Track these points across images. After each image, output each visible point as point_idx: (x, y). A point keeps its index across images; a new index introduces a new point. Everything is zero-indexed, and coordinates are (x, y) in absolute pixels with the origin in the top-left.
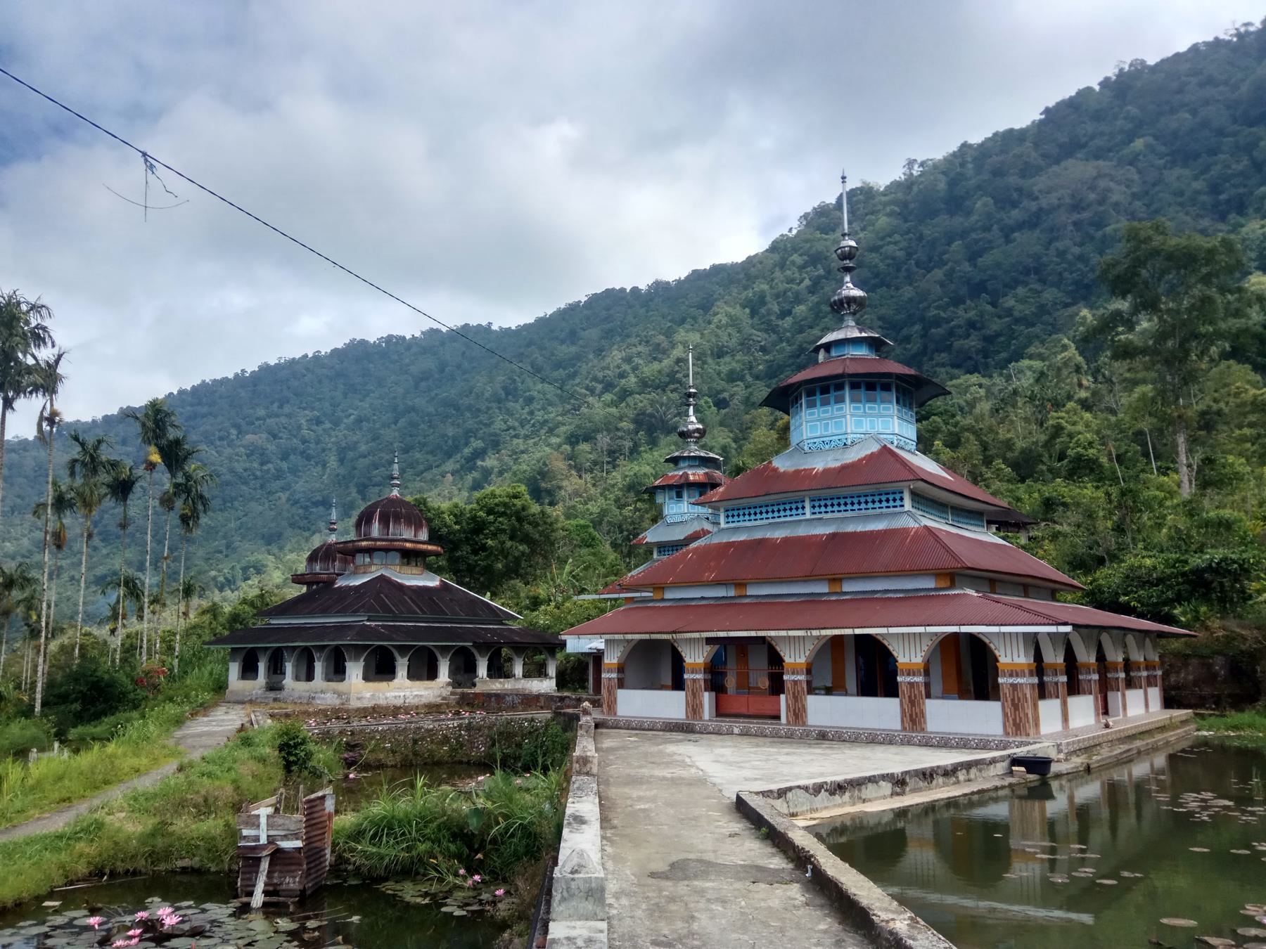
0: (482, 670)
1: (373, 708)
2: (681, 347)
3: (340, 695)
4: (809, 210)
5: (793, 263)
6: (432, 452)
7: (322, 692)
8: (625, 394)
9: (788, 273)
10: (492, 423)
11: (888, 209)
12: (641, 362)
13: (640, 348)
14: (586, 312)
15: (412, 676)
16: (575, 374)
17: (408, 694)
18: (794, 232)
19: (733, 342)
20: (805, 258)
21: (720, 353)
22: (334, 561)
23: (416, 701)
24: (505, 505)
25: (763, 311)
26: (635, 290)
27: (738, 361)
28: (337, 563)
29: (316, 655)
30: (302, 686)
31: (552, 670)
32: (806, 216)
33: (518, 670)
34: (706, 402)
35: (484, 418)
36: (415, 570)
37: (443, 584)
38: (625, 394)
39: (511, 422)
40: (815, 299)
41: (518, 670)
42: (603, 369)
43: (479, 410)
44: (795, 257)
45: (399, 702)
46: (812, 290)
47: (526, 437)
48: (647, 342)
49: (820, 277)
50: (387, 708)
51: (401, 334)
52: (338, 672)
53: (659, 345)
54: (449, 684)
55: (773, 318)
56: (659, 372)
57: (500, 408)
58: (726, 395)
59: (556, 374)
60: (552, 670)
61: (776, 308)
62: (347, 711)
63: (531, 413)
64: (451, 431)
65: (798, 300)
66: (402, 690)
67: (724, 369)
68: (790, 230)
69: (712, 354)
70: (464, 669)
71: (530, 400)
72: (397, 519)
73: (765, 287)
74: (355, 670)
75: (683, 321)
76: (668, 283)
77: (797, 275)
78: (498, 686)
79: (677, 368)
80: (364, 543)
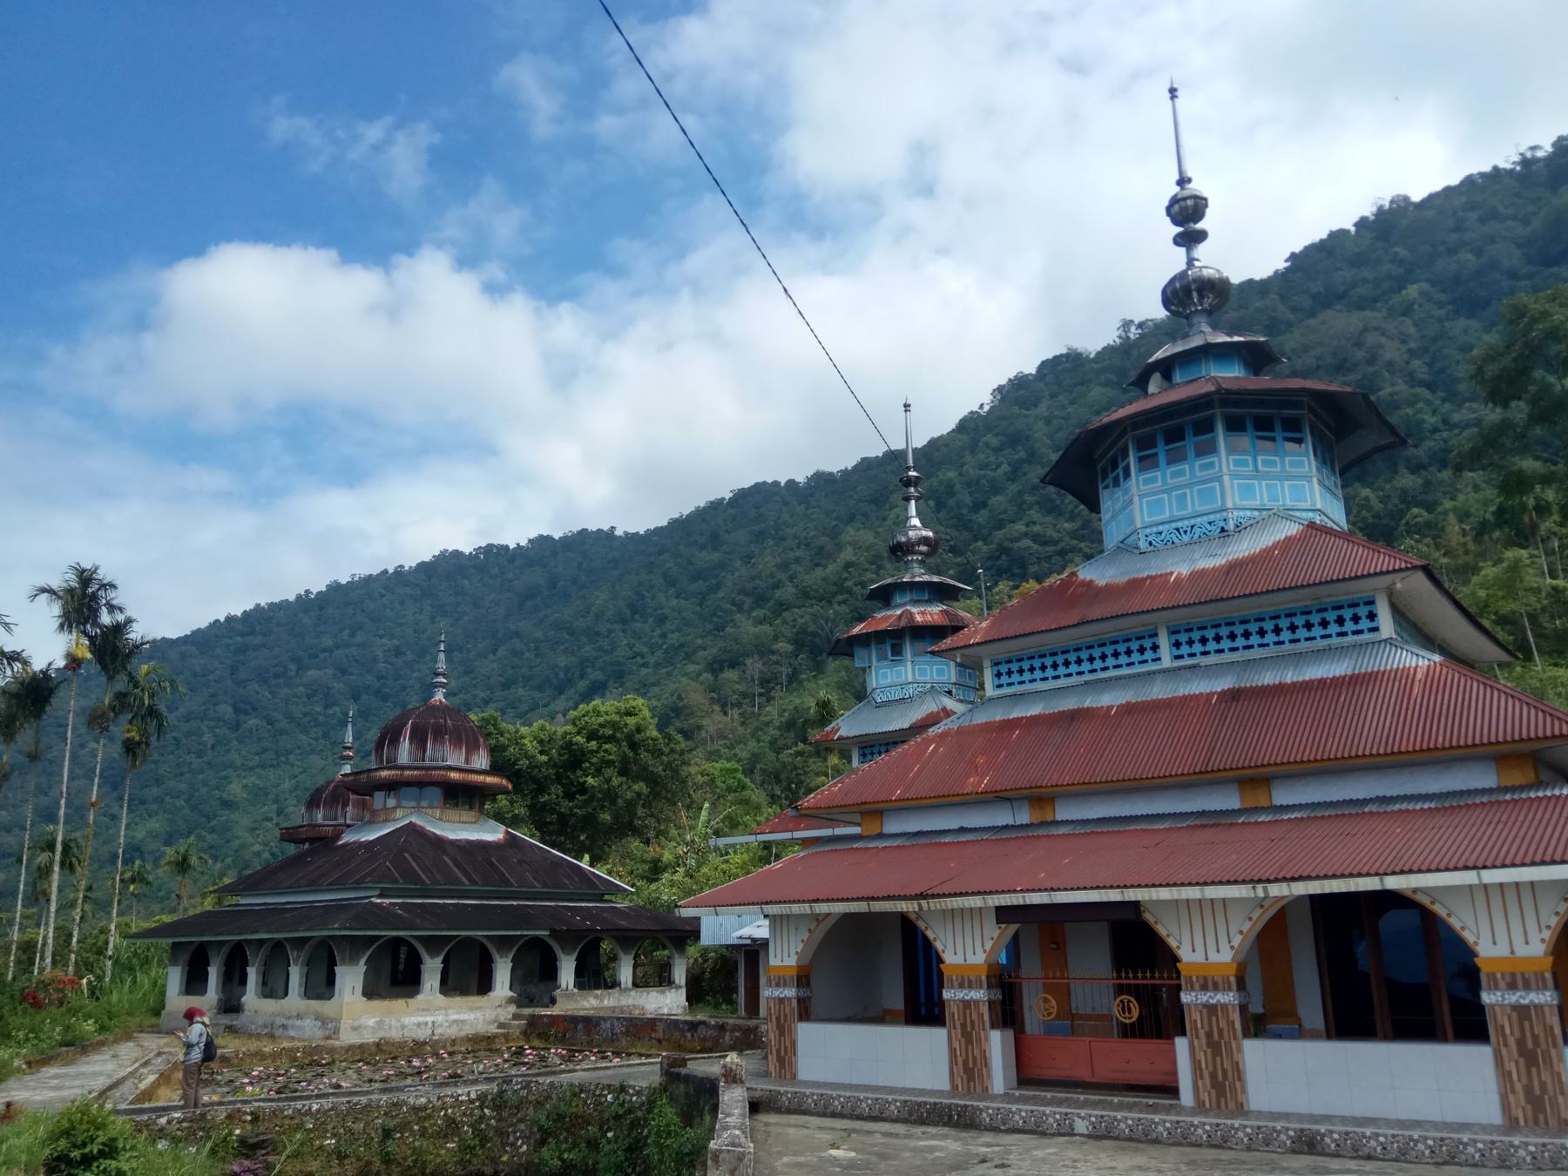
1: (378, 1045)
2: (849, 549)
3: (323, 1020)
4: (1004, 381)
5: (987, 445)
6: (539, 688)
7: (299, 1017)
8: (782, 607)
9: (981, 456)
10: (613, 650)
11: (1102, 378)
13: (799, 553)
14: (732, 511)
15: (450, 986)
16: (718, 586)
17: (440, 1018)
18: (986, 408)
22: (345, 805)
23: (453, 1032)
24: (614, 725)
25: (951, 502)
26: (791, 483)
28: (350, 809)
29: (292, 955)
30: (270, 1005)
31: (680, 974)
32: (1000, 389)
33: (626, 974)
35: (605, 643)
36: (466, 815)
37: (511, 841)
38: (782, 607)
39: (638, 647)
40: (1014, 488)
41: (626, 974)
42: (753, 579)
43: (598, 634)
44: (989, 438)
45: (422, 1035)
46: (1013, 476)
47: (657, 665)
48: (807, 545)
49: (1022, 461)
50: (402, 1045)
52: (322, 985)
53: (822, 548)
54: (510, 1001)
56: (824, 579)
57: (624, 631)
59: (694, 587)
60: (680, 974)
61: (967, 499)
62: (331, 1051)
63: (664, 636)
64: (562, 661)
65: (996, 489)
66: (433, 1014)
68: (981, 406)
71: (662, 620)
72: (439, 734)
73: (952, 474)
74: (350, 978)
75: (851, 519)
76: (831, 474)
77: (992, 459)
78: (592, 1003)
79: (845, 575)
80: (384, 773)
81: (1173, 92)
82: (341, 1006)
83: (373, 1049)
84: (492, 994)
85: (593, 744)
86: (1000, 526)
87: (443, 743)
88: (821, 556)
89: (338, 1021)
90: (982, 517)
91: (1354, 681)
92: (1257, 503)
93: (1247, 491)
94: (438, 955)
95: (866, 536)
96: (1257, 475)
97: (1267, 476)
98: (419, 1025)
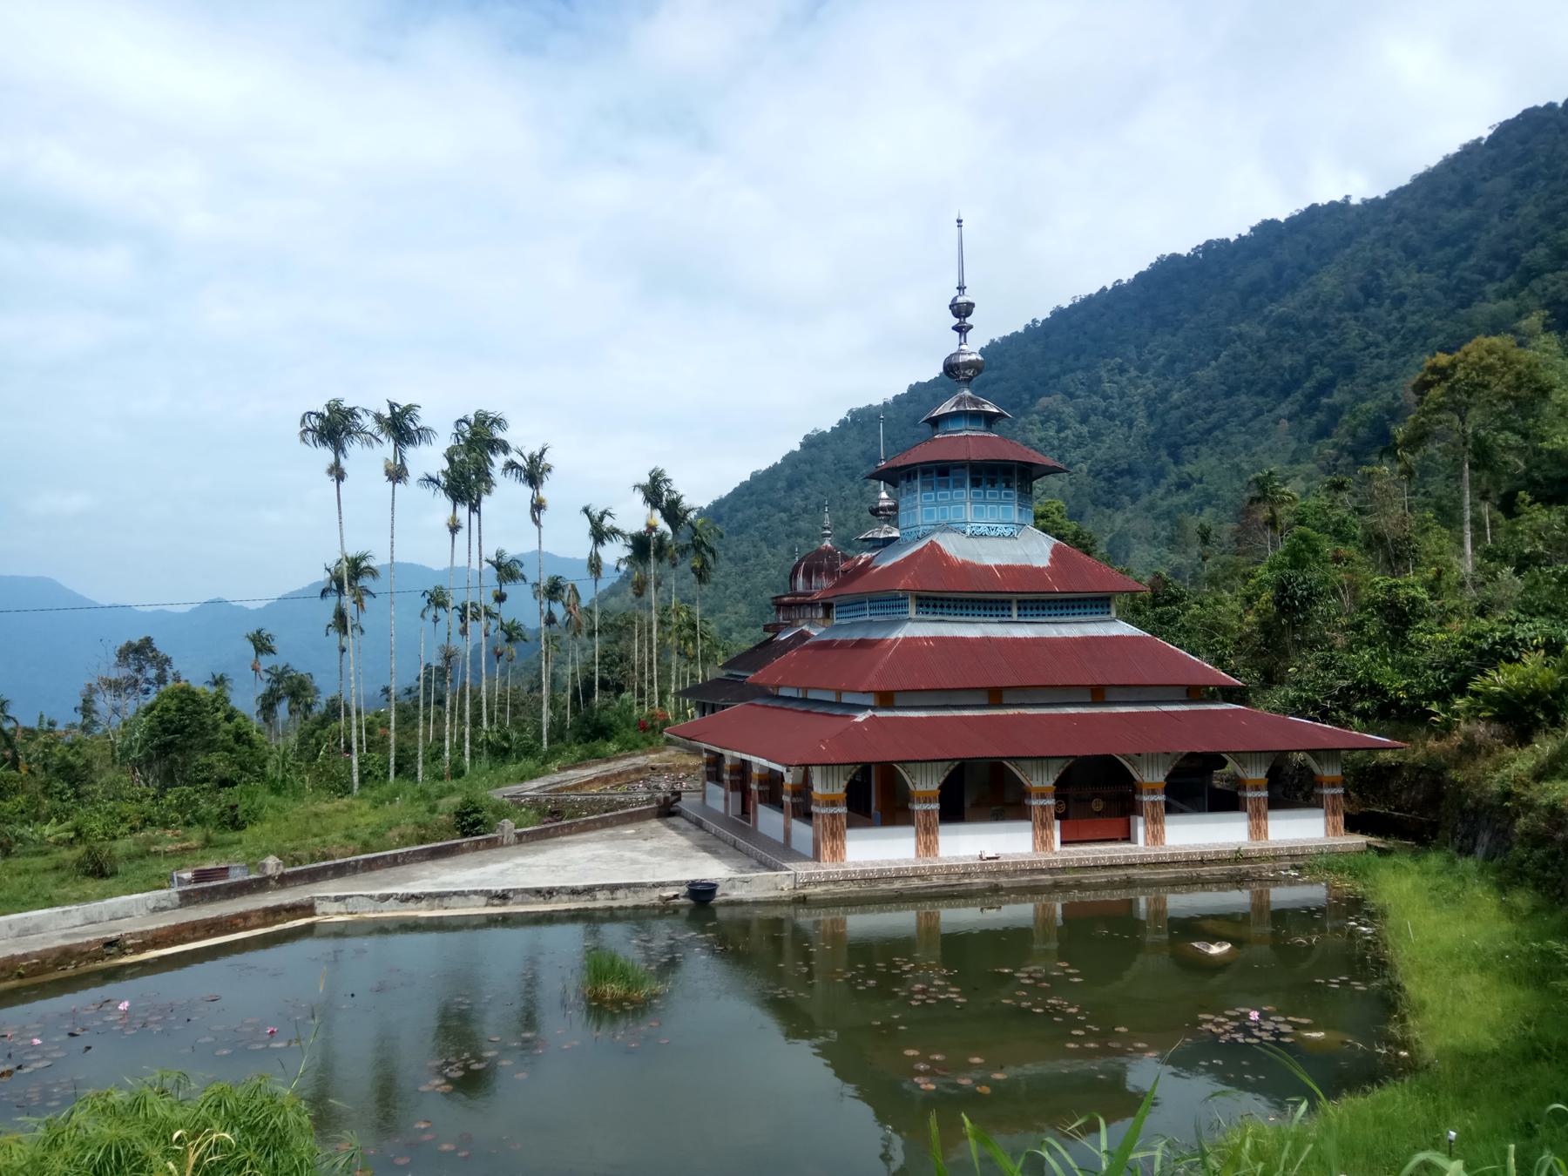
6: (1262, 393)
8: (1531, 273)
10: (1343, 342)
14: (1492, 152)
16: (1469, 251)
35: (1332, 335)
38: (1531, 273)
39: (1372, 336)
43: (1326, 325)
47: (1393, 355)
51: (1223, 236)
57: (1356, 319)
59: (1439, 255)
63: (1402, 319)
64: (1287, 360)
71: (1400, 300)
81: (959, 221)
91: (862, 644)
92: (934, 521)
93: (930, 514)
96: (937, 503)
97: (942, 504)
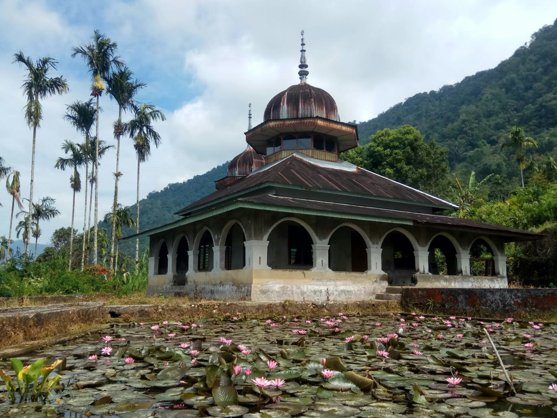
0: (422, 263)
1: (283, 306)
2: (464, 115)
3: (238, 285)
4: (537, 30)
5: (530, 60)
9: (528, 66)
12: (438, 128)
13: (438, 121)
15: (336, 265)
17: (331, 288)
18: (528, 45)
19: (497, 108)
20: (538, 56)
21: (489, 115)
23: (342, 299)
25: (514, 88)
27: (501, 118)
31: (502, 267)
32: (535, 34)
34: (483, 142)
36: (329, 155)
37: (360, 174)
40: (546, 78)
44: (531, 57)
45: (320, 299)
46: (546, 71)
48: (442, 117)
50: (303, 306)
53: (449, 117)
54: (383, 278)
55: (521, 92)
56: (453, 129)
58: (494, 137)
60: (502, 267)
61: (522, 86)
62: (244, 309)
65: (536, 80)
66: (323, 285)
67: (492, 123)
68: (526, 44)
69: (484, 116)
70: (400, 263)
73: (514, 75)
74: (257, 251)
75: (463, 103)
77: (534, 66)
78: (444, 283)
79: (463, 126)
82: (251, 272)
83: (280, 309)
84: (369, 272)
85: (388, 151)
86: (540, 96)
87: (310, 104)
88: (449, 120)
89: (250, 284)
90: (530, 93)
94: (325, 238)
95: (472, 108)
98: (315, 292)
